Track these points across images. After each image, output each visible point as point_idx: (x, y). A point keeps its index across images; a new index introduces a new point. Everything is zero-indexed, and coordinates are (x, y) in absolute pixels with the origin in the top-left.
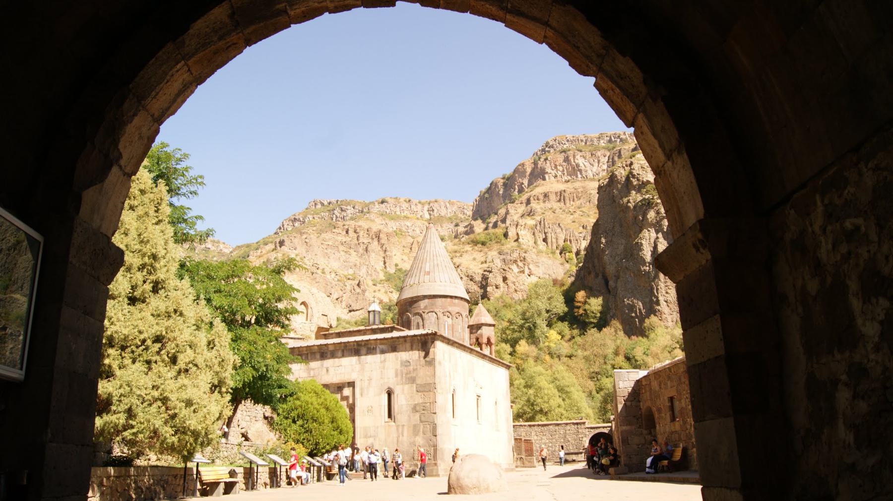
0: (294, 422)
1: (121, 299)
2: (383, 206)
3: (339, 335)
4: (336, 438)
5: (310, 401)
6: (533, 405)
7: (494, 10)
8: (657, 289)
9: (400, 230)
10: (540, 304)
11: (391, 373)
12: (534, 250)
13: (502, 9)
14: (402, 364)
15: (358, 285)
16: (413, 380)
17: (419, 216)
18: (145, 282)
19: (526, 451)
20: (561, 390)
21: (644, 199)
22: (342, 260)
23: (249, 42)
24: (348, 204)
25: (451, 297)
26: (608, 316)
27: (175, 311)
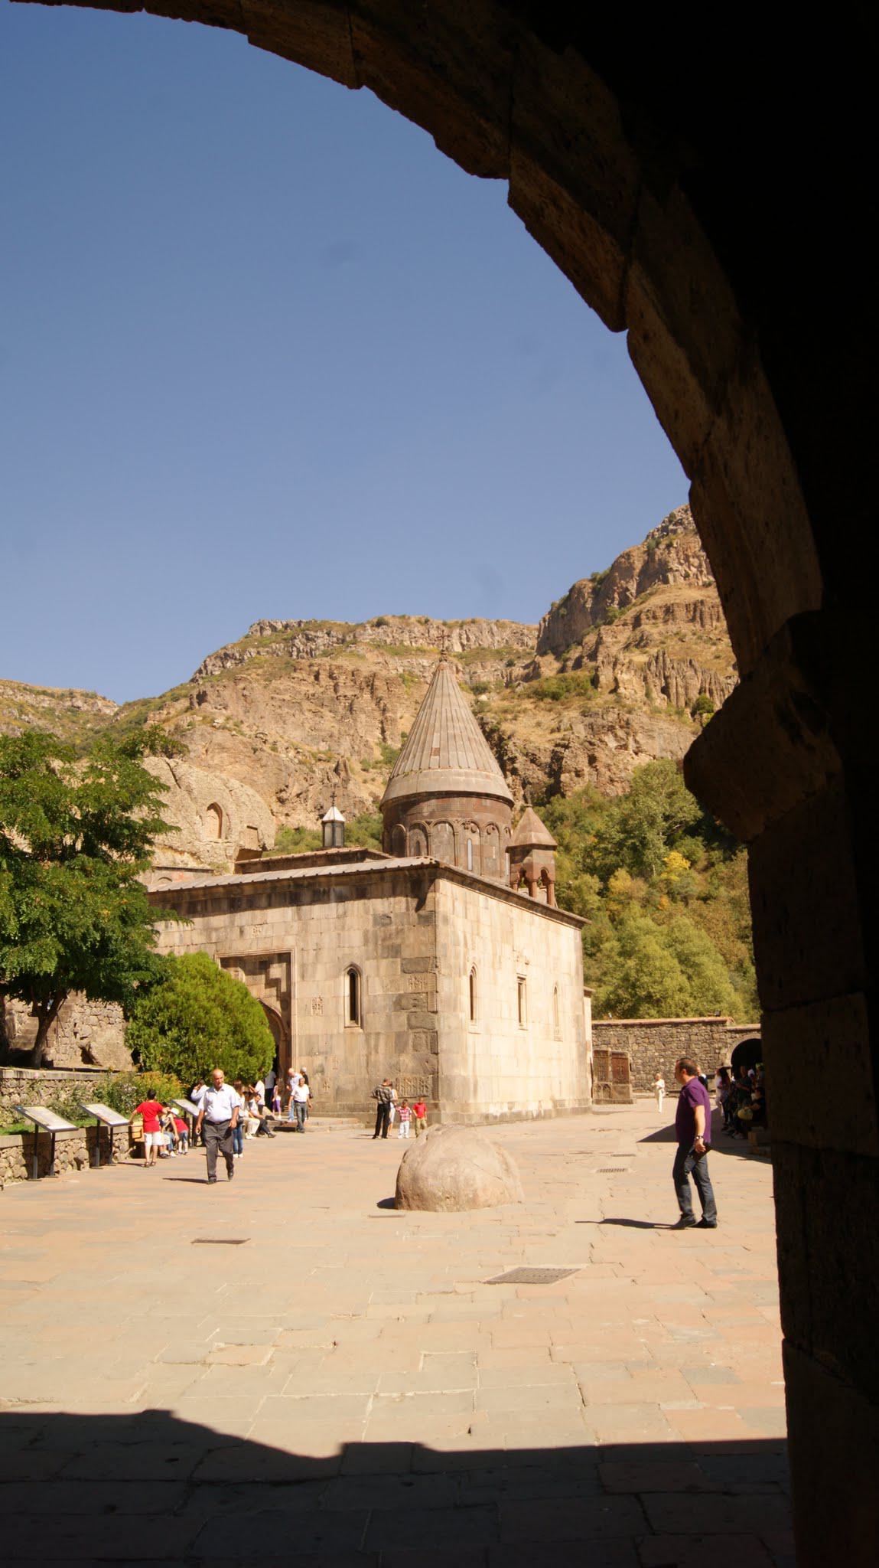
0: (163, 1032)
2: (380, 630)
5: (192, 992)
6: (634, 986)
9: (411, 673)
11: (356, 938)
12: (645, 708)
14: (375, 923)
15: (336, 770)
16: (394, 951)
19: (616, 1073)
20: (684, 959)
22: (307, 726)
24: (319, 627)
25: (479, 795)
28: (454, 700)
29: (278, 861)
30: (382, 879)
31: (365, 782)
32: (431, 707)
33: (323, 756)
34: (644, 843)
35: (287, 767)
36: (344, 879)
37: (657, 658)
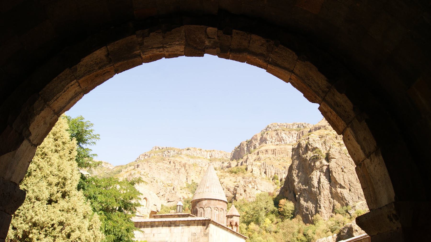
1: (43, 201)
3: (161, 217)
7: (261, 62)
8: (320, 201)
12: (260, 177)
13: (266, 61)
14: (192, 234)
15: (173, 189)
17: (205, 157)
18: (58, 192)
21: (314, 156)
22: (166, 176)
23: (118, 71)
24: (171, 149)
25: (219, 200)
27: (73, 209)
29: (164, 216)
30: (194, 223)
36: (184, 222)
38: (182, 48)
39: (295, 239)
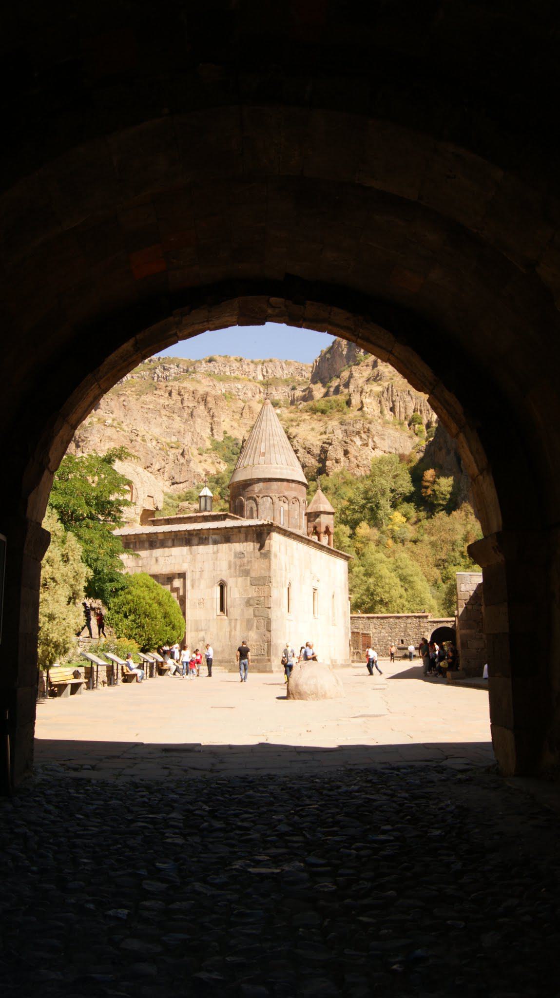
0: (126, 616)
2: (211, 365)
3: (169, 522)
4: (169, 633)
6: (372, 594)
9: (230, 393)
10: (384, 482)
11: (224, 565)
12: (380, 421)
14: (235, 556)
15: (182, 454)
17: (251, 377)
19: (364, 645)
20: (403, 579)
22: (164, 426)
24: (172, 362)
25: (288, 481)
26: (459, 499)
28: (273, 423)
30: (240, 532)
31: (200, 462)
32: (260, 427)
33: (174, 445)
34: (378, 506)
35: (152, 452)
36: (218, 531)
37: (388, 389)
38: (235, 319)
39: (457, 554)
